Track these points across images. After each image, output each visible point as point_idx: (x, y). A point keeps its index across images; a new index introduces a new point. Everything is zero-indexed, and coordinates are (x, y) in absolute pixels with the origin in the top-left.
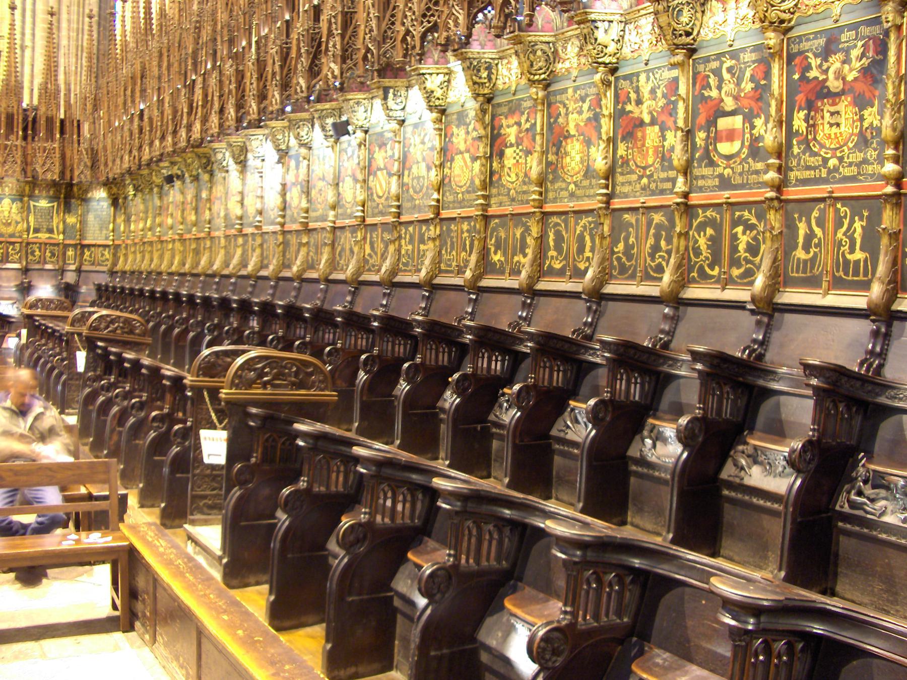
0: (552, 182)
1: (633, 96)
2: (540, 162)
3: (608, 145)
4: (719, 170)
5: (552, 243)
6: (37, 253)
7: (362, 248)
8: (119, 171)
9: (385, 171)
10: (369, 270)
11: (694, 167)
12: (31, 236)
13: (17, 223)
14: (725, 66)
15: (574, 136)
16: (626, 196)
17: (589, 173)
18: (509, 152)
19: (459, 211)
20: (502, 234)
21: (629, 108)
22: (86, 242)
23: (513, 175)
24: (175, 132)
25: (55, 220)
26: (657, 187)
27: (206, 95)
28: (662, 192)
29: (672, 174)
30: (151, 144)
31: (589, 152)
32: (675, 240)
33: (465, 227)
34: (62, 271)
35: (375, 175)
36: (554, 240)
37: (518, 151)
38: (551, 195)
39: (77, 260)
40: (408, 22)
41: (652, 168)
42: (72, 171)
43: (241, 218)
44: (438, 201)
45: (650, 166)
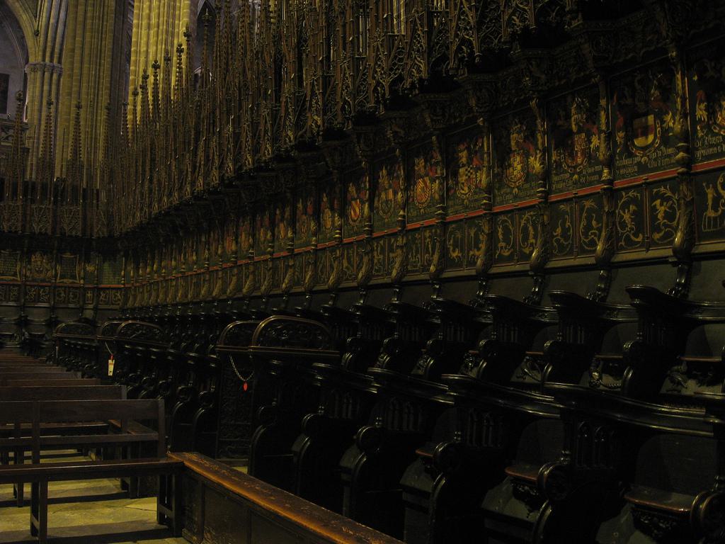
0: (499, 189)
1: (562, 113)
2: (488, 175)
3: (544, 154)
4: (637, 160)
5: (501, 237)
6: (63, 295)
7: (341, 263)
8: (131, 226)
9: (358, 200)
10: (347, 279)
11: (616, 160)
12: (58, 281)
13: (47, 270)
14: (637, 79)
15: (515, 151)
16: (561, 191)
17: (528, 176)
18: (461, 170)
19: (421, 222)
20: (459, 236)
21: (560, 123)
22: (102, 286)
23: (466, 189)
24: (180, 189)
25: (77, 268)
26: (586, 179)
27: (207, 157)
28: (591, 183)
29: (598, 168)
30: (160, 201)
31: (528, 162)
32: (605, 218)
33: (427, 234)
34: (82, 309)
35: (351, 204)
36: (503, 234)
37: (469, 169)
38: (498, 199)
39: (95, 299)
40: (378, 76)
41: (581, 166)
42: (92, 229)
43: (236, 253)
44: (404, 217)
45: (580, 165)
